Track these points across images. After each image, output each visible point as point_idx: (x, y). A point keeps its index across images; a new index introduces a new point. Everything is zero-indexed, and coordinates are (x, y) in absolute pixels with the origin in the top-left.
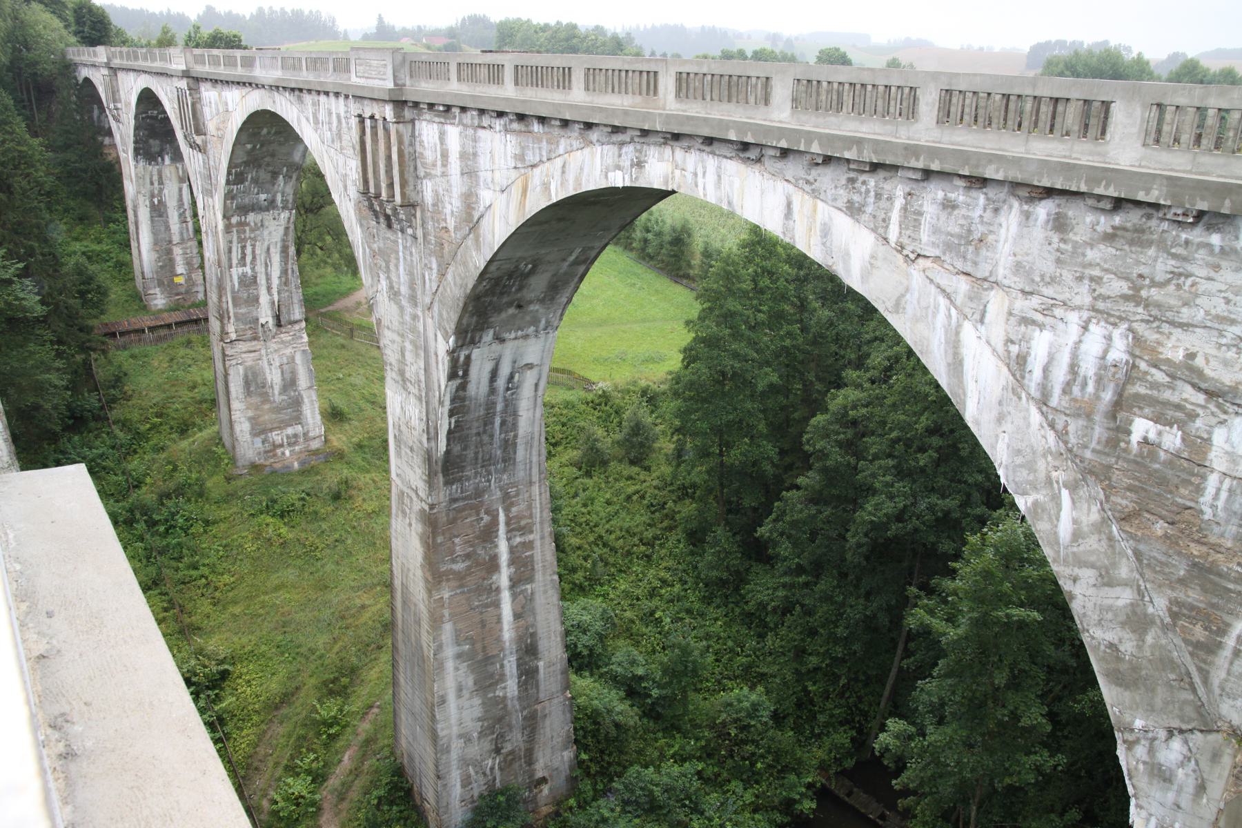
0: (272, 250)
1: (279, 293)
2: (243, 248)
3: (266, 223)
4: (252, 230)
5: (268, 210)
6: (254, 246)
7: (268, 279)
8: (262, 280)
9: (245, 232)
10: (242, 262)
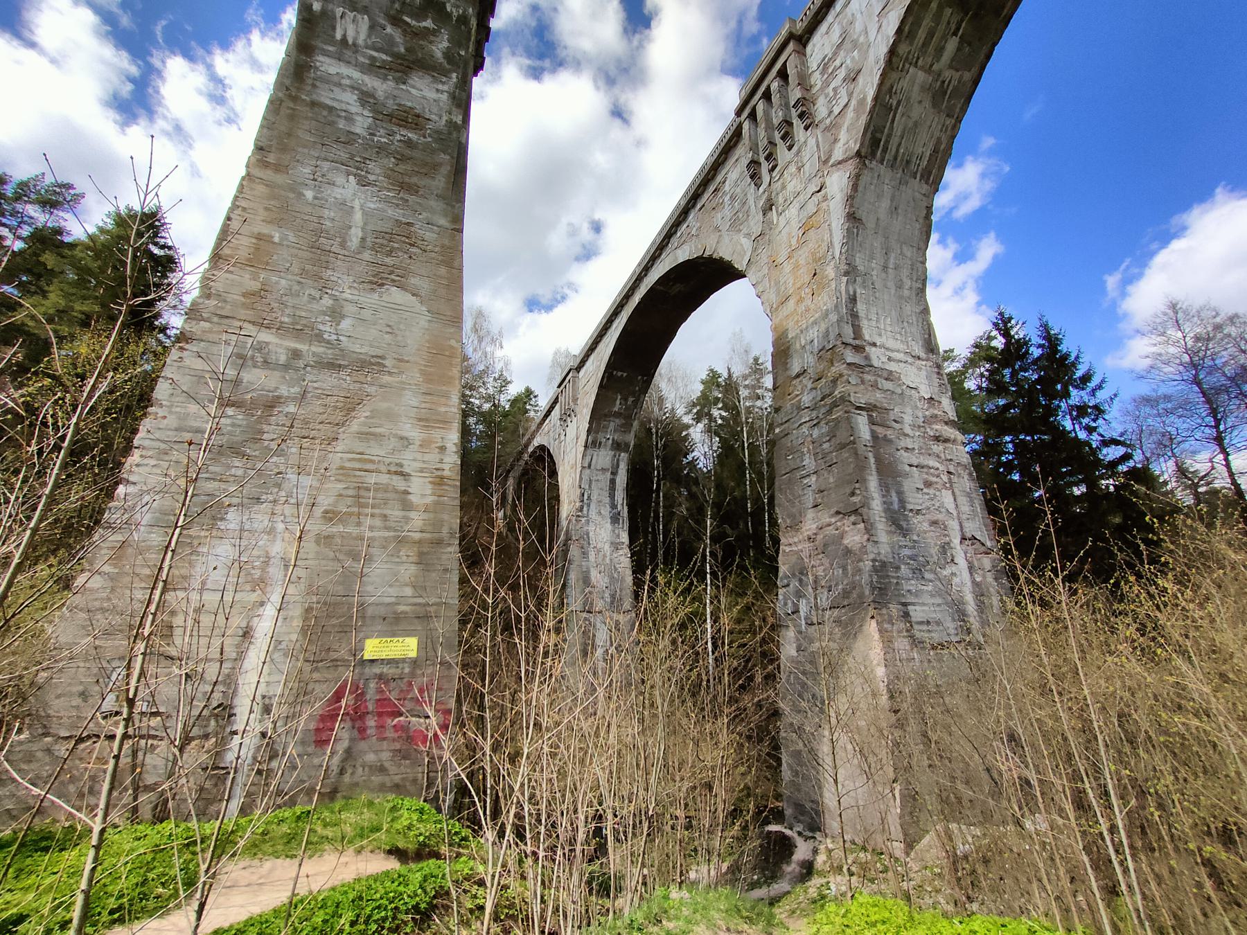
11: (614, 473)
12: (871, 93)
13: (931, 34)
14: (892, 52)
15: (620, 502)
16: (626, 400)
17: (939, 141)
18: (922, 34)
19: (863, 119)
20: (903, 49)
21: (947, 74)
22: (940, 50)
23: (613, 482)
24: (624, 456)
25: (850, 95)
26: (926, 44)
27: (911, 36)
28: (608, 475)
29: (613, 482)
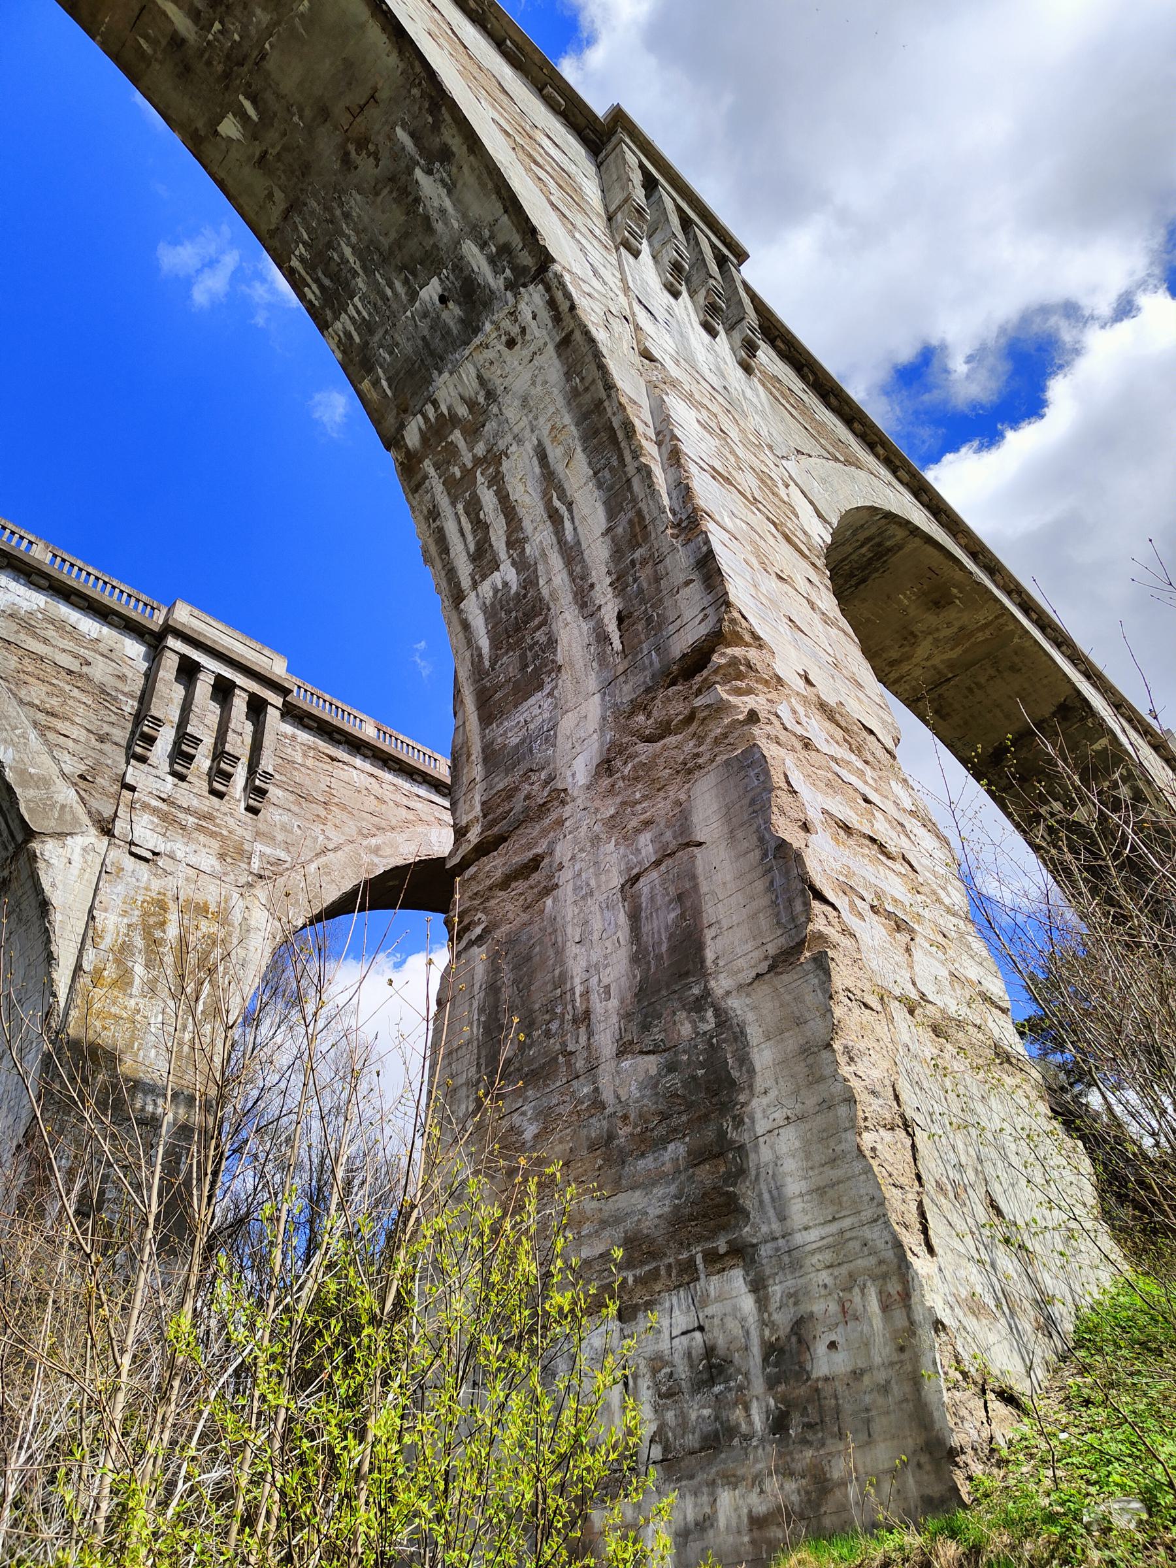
0: (555, 453)
1: (619, 584)
2: (474, 508)
3: (494, 375)
4: (473, 432)
5: (471, 327)
6: (497, 481)
7: (572, 554)
8: (555, 578)
9: (452, 449)
10: (483, 559)
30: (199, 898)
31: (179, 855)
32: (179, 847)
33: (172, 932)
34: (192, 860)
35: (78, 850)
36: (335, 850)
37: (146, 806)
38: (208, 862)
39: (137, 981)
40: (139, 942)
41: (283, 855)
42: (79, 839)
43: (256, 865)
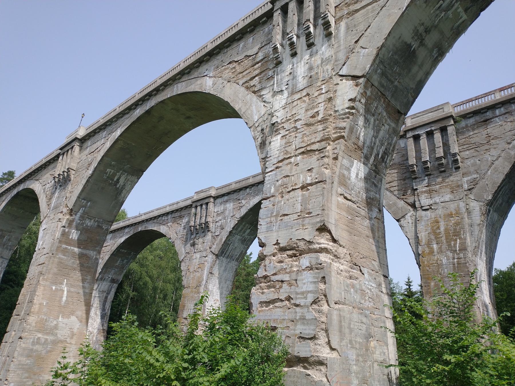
11: (108, 294)
12: (224, 240)
13: (242, 229)
14: (231, 232)
15: (107, 308)
16: (123, 261)
17: (242, 251)
18: (239, 229)
19: (220, 246)
20: (234, 232)
21: (247, 236)
22: (244, 232)
23: (106, 298)
24: (116, 286)
25: (220, 233)
26: (241, 231)
27: (237, 229)
28: (105, 294)
29: (106, 298)
30: (448, 212)
31: (438, 201)
32: (437, 199)
33: (442, 229)
34: (442, 200)
35: (409, 218)
36: (497, 159)
37: (422, 192)
38: (448, 197)
39: (435, 250)
40: (433, 237)
41: (475, 176)
42: (409, 214)
43: (466, 186)
